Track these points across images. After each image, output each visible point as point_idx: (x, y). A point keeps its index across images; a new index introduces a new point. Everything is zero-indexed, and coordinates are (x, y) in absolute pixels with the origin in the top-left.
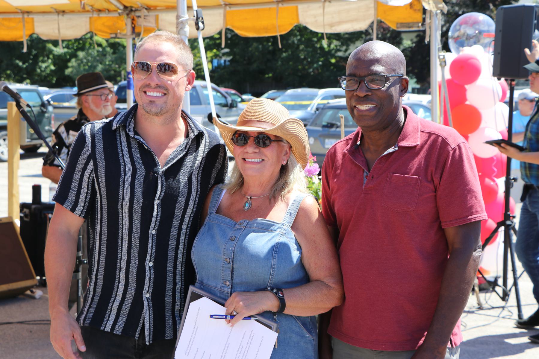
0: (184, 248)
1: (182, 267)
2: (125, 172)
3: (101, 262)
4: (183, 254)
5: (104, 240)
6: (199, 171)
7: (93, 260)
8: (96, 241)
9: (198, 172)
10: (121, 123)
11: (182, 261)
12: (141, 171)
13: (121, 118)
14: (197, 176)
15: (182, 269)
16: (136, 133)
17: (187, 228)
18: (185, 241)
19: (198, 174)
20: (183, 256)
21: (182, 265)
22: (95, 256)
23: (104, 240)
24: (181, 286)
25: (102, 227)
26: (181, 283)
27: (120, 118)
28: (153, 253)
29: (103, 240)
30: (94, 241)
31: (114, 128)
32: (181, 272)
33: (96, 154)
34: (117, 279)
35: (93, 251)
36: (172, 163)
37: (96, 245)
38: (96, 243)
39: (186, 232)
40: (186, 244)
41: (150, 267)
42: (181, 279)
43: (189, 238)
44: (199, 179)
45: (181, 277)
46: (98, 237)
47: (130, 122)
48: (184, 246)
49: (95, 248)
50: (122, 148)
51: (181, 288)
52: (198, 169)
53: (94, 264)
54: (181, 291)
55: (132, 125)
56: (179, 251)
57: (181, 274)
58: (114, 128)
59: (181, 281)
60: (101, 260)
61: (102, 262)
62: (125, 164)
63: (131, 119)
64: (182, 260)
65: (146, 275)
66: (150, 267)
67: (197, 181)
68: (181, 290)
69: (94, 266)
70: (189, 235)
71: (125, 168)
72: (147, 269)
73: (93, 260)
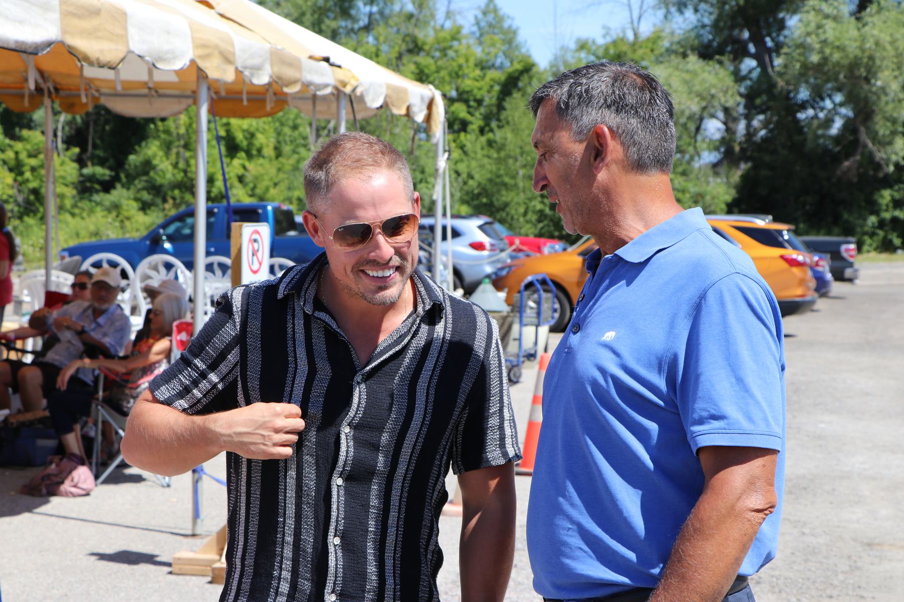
0: (399, 517)
1: (395, 550)
2: (295, 375)
3: (251, 534)
4: (397, 527)
5: (257, 494)
6: (432, 376)
7: (236, 531)
8: (240, 495)
9: (431, 378)
10: (291, 288)
11: (396, 540)
12: (325, 371)
13: (293, 278)
14: (428, 387)
15: (395, 553)
16: (318, 305)
17: (404, 480)
18: (400, 503)
19: (430, 383)
20: (397, 530)
21: (395, 547)
22: (239, 522)
23: (257, 494)
24: (395, 586)
25: (251, 470)
26: (394, 579)
27: (292, 279)
28: (341, 521)
29: (255, 494)
30: (237, 496)
31: (280, 295)
32: (394, 559)
33: (247, 338)
34: (277, 563)
35: (237, 514)
36: (382, 359)
37: (240, 502)
38: (240, 498)
39: (403, 486)
40: (403, 510)
41: (335, 546)
42: (394, 573)
43: (408, 498)
44: (432, 391)
45: (394, 570)
46: (243, 489)
47: (309, 286)
48: (399, 513)
49: (240, 509)
50: (294, 331)
51: (395, 589)
52: (430, 373)
53: (238, 539)
54: (394, 595)
55: (311, 293)
56: (390, 522)
57: (394, 563)
58: (280, 295)
59: (394, 576)
60: (251, 531)
61: (251, 534)
62: (296, 359)
63: (311, 282)
64: (396, 538)
65: (330, 561)
66: (335, 546)
67: (427, 396)
68: (395, 592)
69: (238, 542)
70: (409, 492)
71: (296, 368)
72: (331, 549)
73: (236, 531)
